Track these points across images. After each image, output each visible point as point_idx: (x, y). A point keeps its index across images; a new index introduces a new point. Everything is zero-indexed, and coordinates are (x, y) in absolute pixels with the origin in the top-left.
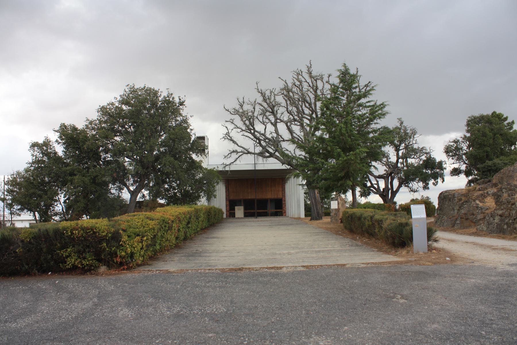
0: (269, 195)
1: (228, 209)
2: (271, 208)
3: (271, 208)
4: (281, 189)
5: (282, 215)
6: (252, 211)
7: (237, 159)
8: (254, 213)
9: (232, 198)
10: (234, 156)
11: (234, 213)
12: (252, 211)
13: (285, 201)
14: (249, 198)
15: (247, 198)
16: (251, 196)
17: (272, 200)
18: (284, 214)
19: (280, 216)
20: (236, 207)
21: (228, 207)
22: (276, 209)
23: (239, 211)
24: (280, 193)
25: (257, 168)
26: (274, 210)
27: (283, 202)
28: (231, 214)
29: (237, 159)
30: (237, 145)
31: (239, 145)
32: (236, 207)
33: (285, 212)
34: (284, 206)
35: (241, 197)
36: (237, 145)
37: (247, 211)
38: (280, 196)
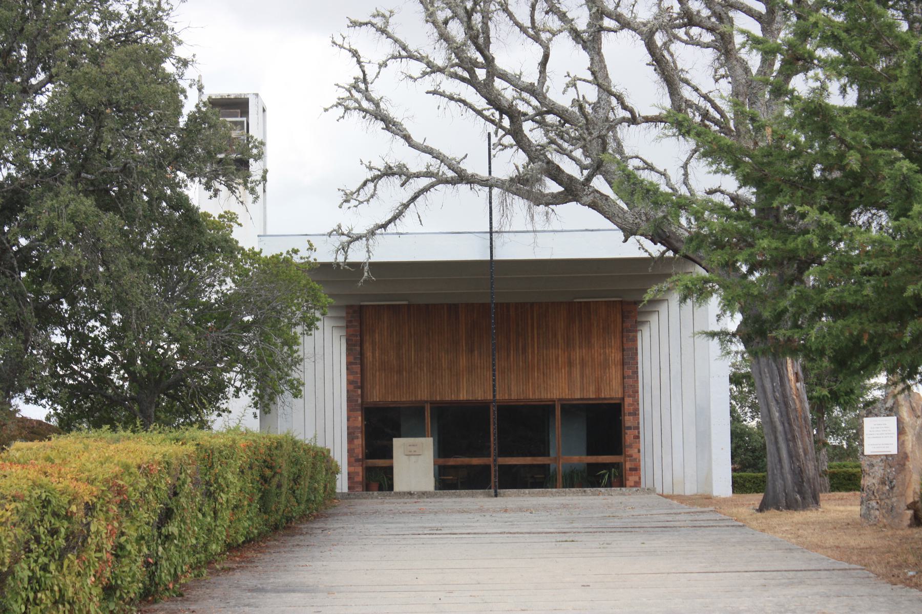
0: (561, 384)
1: (359, 452)
2: (567, 451)
3: (567, 451)
4: (615, 355)
5: (622, 484)
6: (475, 461)
7: (406, 206)
9: (376, 396)
10: (392, 193)
11: (389, 471)
12: (475, 461)
13: (635, 413)
14: (463, 396)
16: (471, 389)
17: (571, 409)
18: (631, 479)
19: (610, 485)
20: (397, 443)
21: (359, 442)
22: (590, 452)
23: (414, 461)
24: (615, 373)
25: (499, 255)
26: (580, 459)
27: (628, 421)
28: (376, 477)
29: (406, 206)
30: (407, 138)
31: (417, 138)
32: (397, 443)
33: (636, 469)
34: (628, 437)
35: (424, 390)
36: (407, 138)
37: (452, 461)
38: (612, 391)
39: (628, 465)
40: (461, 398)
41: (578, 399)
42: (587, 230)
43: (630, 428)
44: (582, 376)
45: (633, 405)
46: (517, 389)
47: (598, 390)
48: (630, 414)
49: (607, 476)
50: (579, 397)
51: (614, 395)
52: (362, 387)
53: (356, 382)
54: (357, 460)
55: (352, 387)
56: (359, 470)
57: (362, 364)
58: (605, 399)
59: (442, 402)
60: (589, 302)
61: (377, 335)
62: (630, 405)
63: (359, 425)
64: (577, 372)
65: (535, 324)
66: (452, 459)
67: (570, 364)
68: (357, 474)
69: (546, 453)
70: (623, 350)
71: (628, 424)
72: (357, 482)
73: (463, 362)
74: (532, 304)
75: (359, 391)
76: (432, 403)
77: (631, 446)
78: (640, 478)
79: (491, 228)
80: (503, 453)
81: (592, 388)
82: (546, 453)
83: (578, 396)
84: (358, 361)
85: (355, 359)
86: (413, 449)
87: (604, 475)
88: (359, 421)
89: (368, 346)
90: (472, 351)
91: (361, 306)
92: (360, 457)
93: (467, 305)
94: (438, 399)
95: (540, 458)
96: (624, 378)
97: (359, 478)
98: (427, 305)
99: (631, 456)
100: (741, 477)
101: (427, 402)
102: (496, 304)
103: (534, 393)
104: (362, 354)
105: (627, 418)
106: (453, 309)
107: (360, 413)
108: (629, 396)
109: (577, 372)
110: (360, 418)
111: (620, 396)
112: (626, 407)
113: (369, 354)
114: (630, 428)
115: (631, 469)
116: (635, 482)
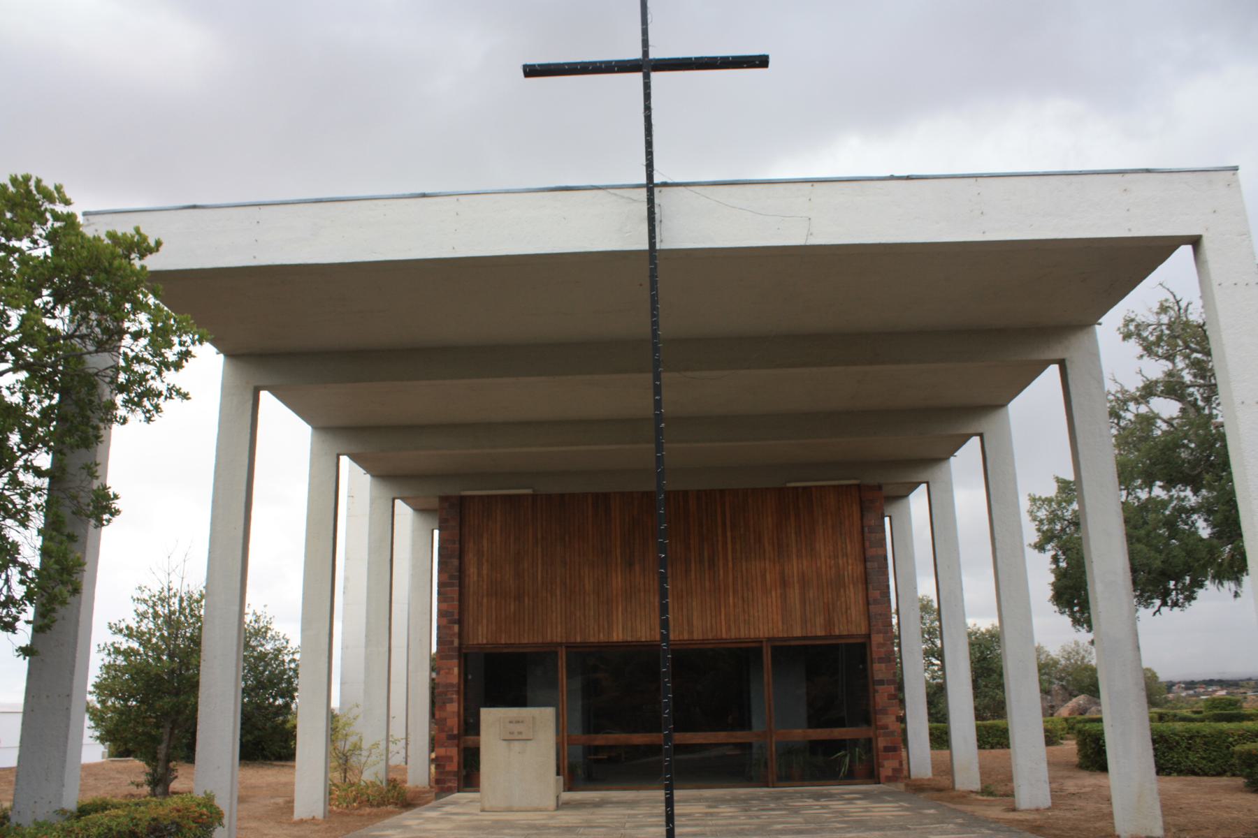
2: (778, 717)
3: (778, 717)
4: (852, 568)
5: (872, 776)
6: (638, 739)
8: (654, 749)
9: (482, 635)
12: (638, 739)
14: (618, 635)
15: (595, 635)
16: (630, 625)
18: (888, 767)
19: (850, 777)
22: (815, 720)
24: (853, 596)
26: (801, 734)
27: (879, 670)
32: (490, 717)
34: (881, 695)
35: (554, 627)
37: (600, 740)
38: (850, 624)
39: (882, 743)
40: (615, 639)
42: (892, 178)
43: (881, 682)
44: (803, 602)
45: (884, 645)
46: (701, 621)
48: (881, 660)
49: (847, 759)
50: (799, 634)
51: (854, 630)
52: (460, 622)
53: (452, 614)
54: (451, 737)
55: (445, 621)
56: (453, 752)
57: (461, 586)
58: (840, 637)
60: (810, 488)
61: (485, 543)
62: (880, 645)
63: (455, 680)
64: (794, 594)
66: (600, 736)
67: (784, 583)
68: (450, 758)
69: (744, 723)
70: (865, 561)
71: (878, 676)
72: (449, 773)
73: (617, 581)
74: (722, 492)
75: (456, 628)
76: (569, 646)
77: (884, 711)
78: (901, 764)
79: (650, 176)
80: (681, 726)
81: (820, 620)
82: (744, 723)
83: (798, 632)
84: (456, 582)
85: (451, 577)
86: (519, 728)
87: (845, 756)
88: (454, 674)
89: (471, 558)
91: (462, 499)
92: (456, 732)
94: (579, 640)
95: (739, 733)
96: (868, 603)
97: (453, 766)
98: (562, 496)
99: (885, 727)
100: (937, 728)
101: (561, 644)
102: (668, 493)
103: (729, 629)
104: (461, 570)
105: (876, 666)
106: (602, 501)
107: (456, 661)
108: (879, 632)
109: (794, 594)
110: (456, 670)
111: (863, 630)
112: (874, 648)
113: (472, 571)
114: (881, 682)
115: (887, 749)
116: (894, 770)
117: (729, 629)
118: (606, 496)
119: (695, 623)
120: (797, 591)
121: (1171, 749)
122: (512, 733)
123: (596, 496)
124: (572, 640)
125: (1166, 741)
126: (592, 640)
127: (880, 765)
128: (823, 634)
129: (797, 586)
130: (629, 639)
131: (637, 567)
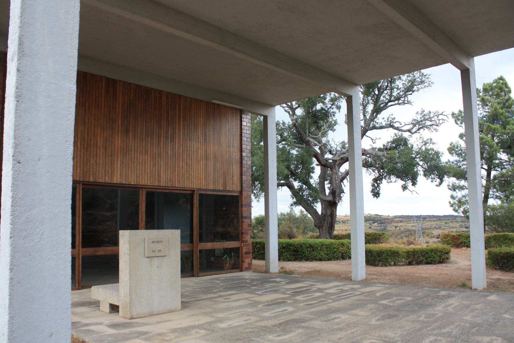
14: (117, 179)
15: (103, 178)
32: (126, 238)
40: (115, 182)
41: (211, 190)
47: (225, 184)
58: (229, 191)
59: (95, 184)
65: (182, 116)
66: (101, 248)
73: (118, 141)
74: (180, 96)
81: (221, 181)
86: (159, 246)
90: (127, 132)
93: (125, 83)
94: (91, 180)
99: (246, 241)
103: (179, 182)
117: (179, 182)
118: (114, 81)
119: (162, 175)
120: (212, 163)
121: (313, 250)
122: (154, 251)
123: (108, 80)
124: (87, 180)
125: (312, 247)
126: (100, 181)
127: (243, 261)
128: (222, 189)
129: (212, 160)
130: (124, 182)
131: (131, 134)
